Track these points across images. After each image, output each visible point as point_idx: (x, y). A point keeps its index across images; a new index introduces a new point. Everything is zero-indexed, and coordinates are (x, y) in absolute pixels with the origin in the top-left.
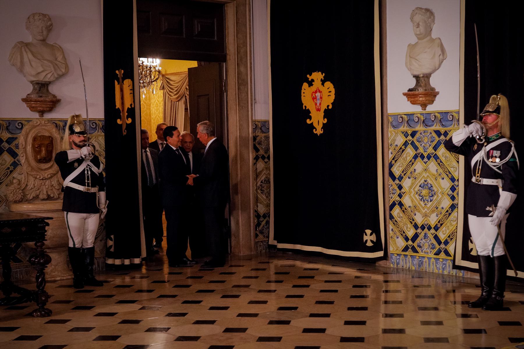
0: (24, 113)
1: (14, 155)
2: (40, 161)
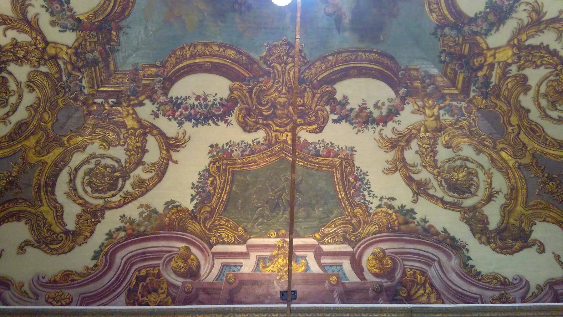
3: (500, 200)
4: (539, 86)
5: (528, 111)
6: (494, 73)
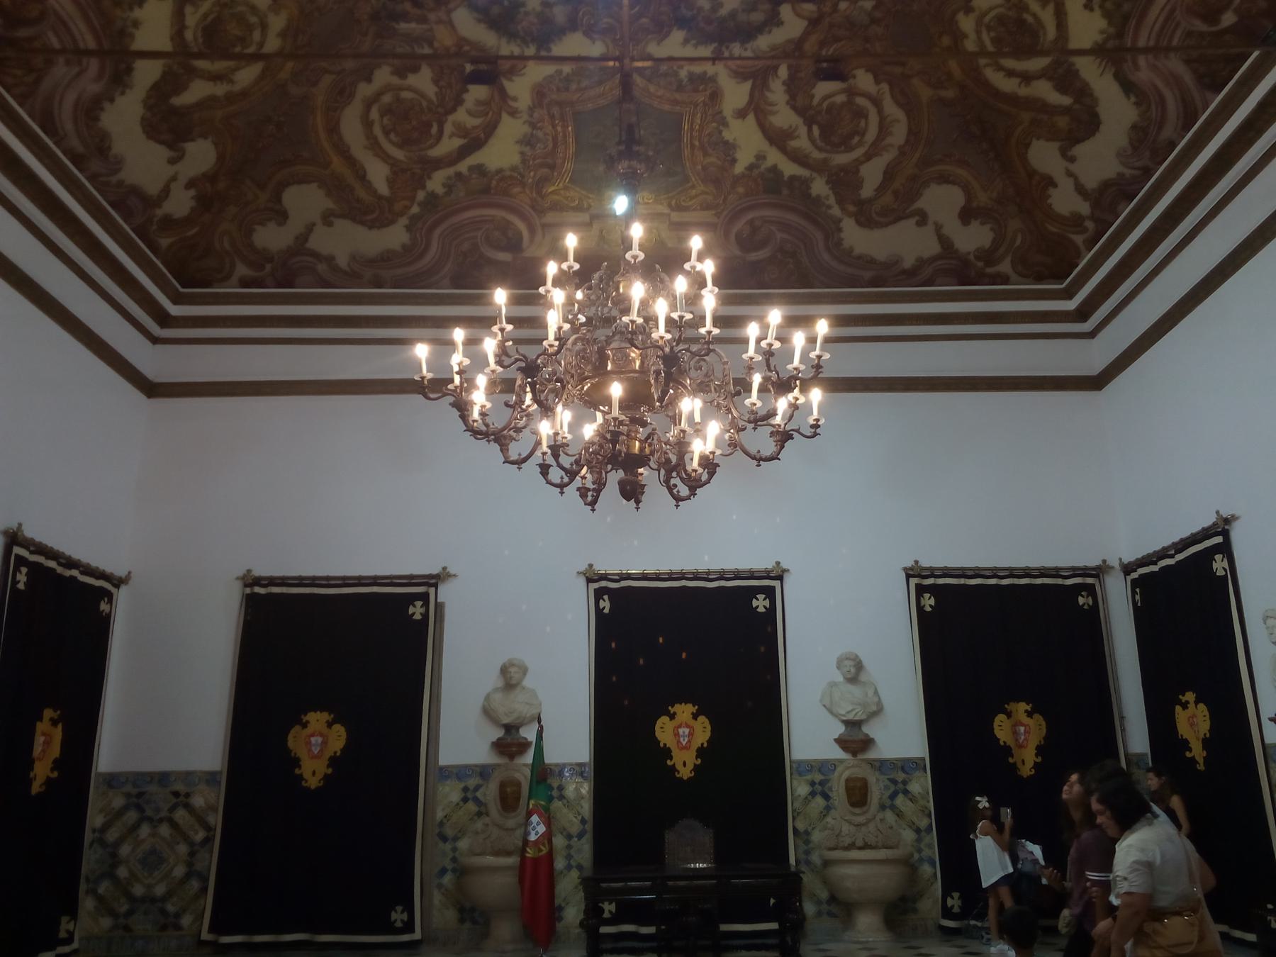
0: (838, 753)
1: (826, 797)
2: (853, 804)
3: (220, 90)
4: (410, 89)
5: (369, 80)
6: (413, 25)
